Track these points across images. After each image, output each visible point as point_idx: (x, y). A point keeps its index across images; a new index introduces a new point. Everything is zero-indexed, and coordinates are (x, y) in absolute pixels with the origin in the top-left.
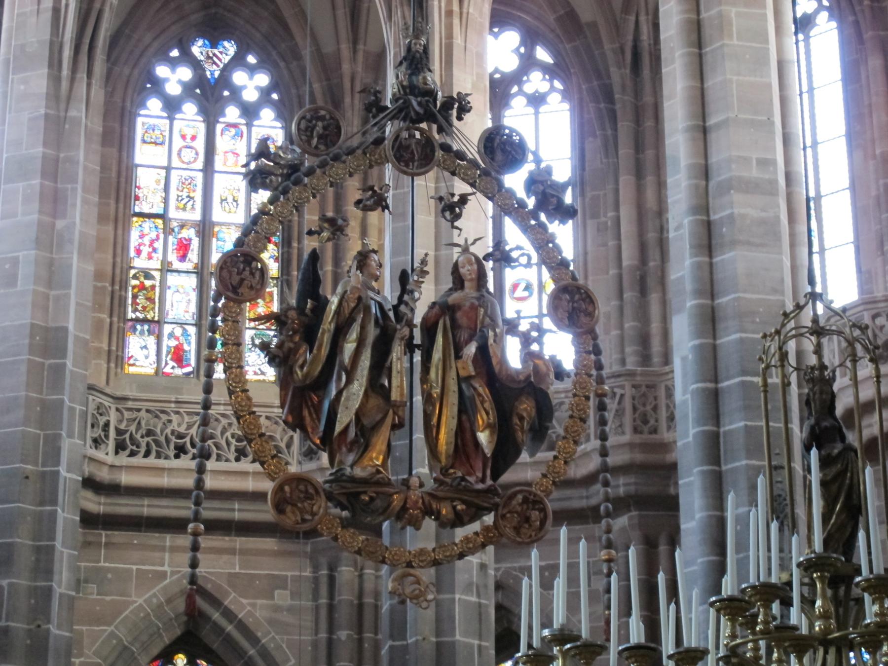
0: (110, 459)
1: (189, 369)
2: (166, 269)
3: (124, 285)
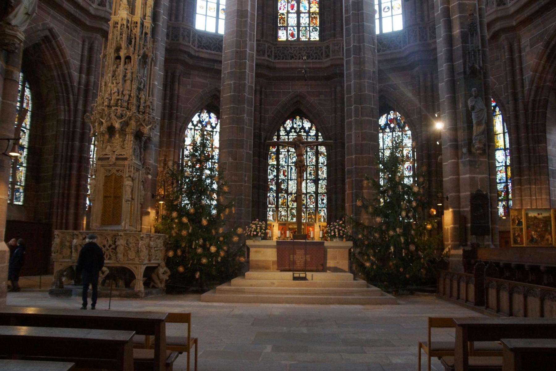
0: (273, 61)
1: (295, 39)
2: (288, 12)
3: (277, 18)
